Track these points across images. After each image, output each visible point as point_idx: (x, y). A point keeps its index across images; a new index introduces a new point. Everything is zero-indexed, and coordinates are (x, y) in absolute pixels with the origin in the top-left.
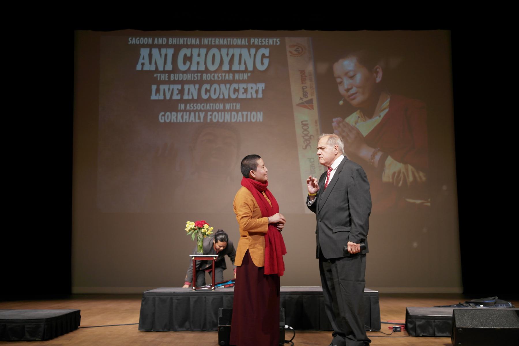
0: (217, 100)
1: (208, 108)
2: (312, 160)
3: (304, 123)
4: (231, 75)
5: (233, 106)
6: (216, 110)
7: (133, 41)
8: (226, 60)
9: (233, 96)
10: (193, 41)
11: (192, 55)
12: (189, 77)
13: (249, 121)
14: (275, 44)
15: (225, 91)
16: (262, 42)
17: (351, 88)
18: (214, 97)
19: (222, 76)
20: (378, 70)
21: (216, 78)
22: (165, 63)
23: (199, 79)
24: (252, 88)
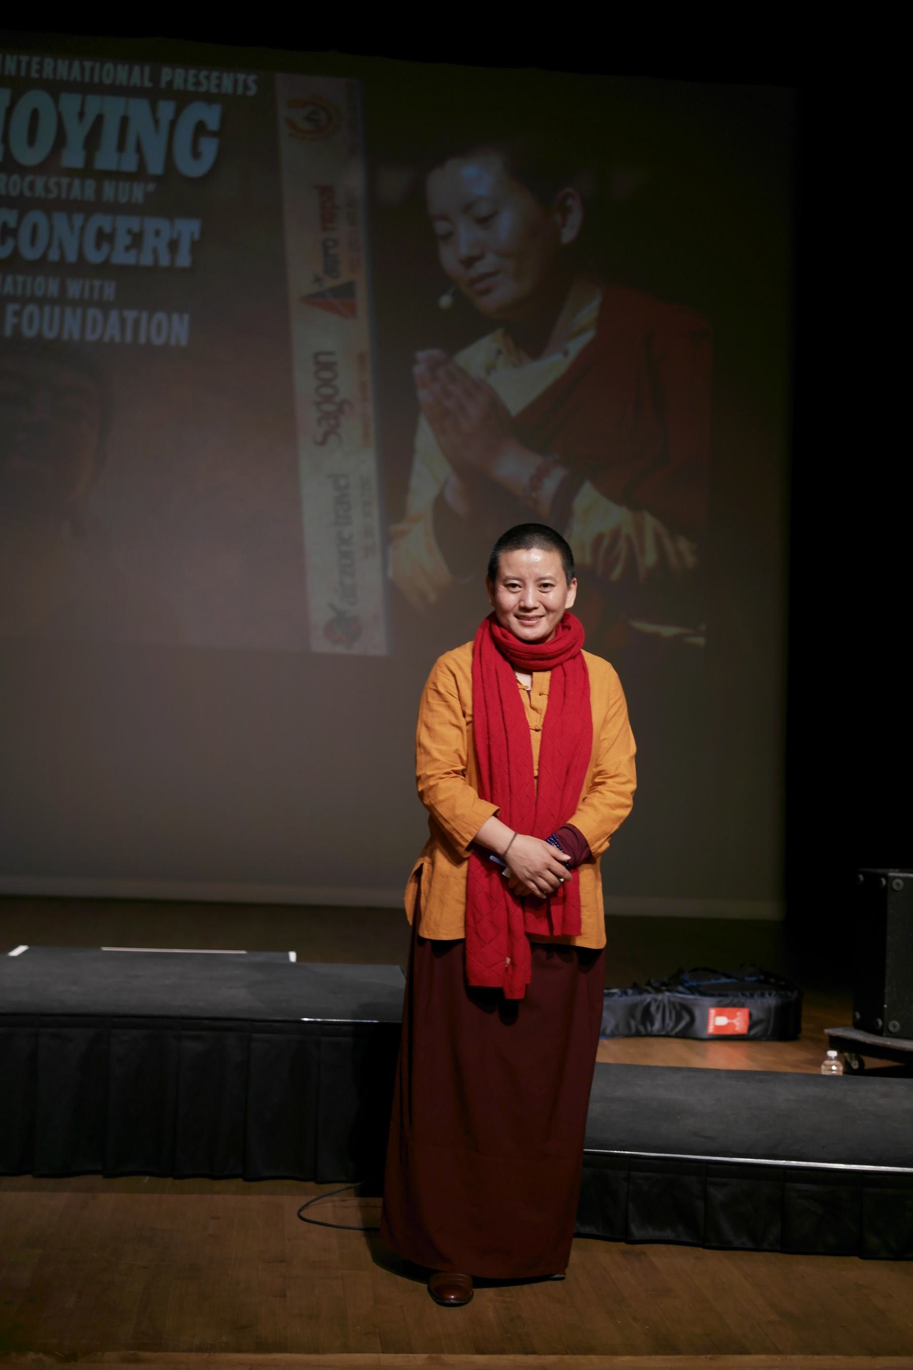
0: (40, 266)
2: (342, 482)
3: (323, 359)
5: (92, 288)
6: (33, 299)
8: (77, 133)
9: (94, 256)
13: (142, 340)
14: (240, 91)
15: (67, 237)
16: (197, 83)
18: (30, 254)
19: (58, 185)
20: (570, 202)
21: (39, 191)
24: (157, 233)
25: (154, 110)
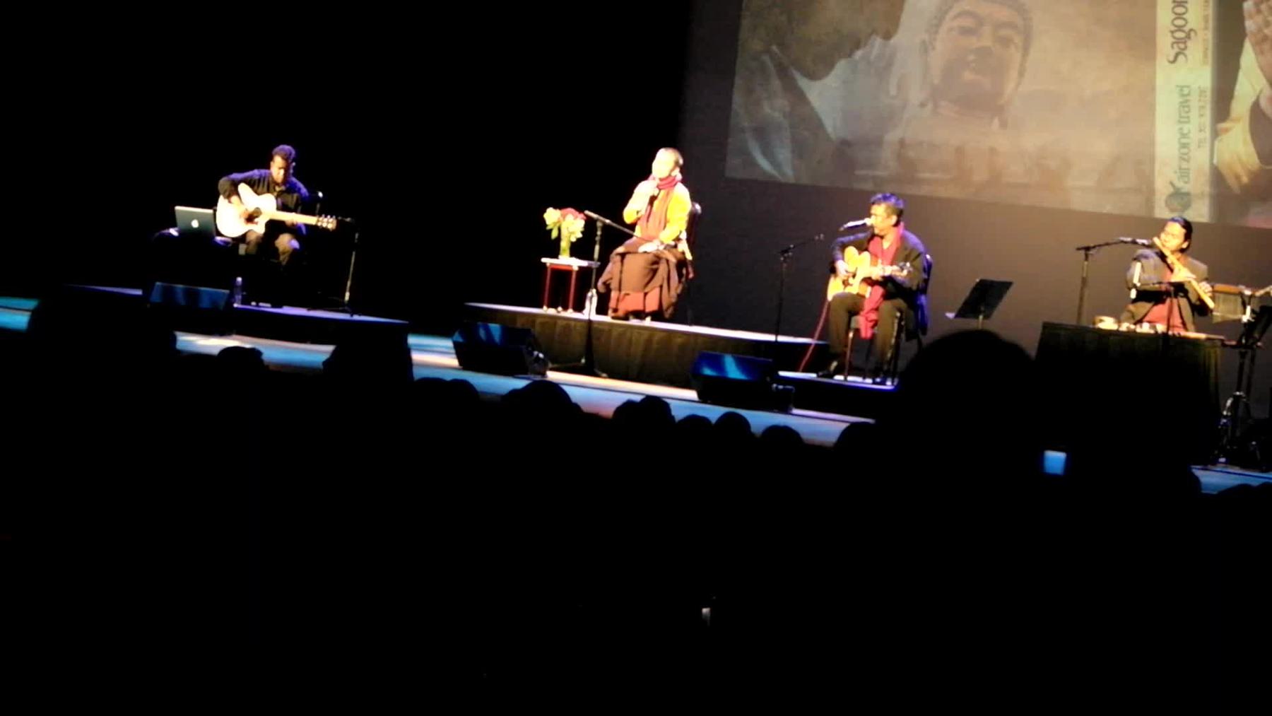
2: (1186, 91)
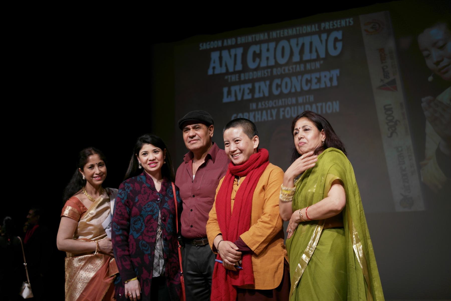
0: (290, 95)
1: (280, 103)
2: (400, 149)
3: (387, 107)
4: (302, 66)
5: (306, 98)
6: (288, 106)
7: (204, 46)
8: (296, 51)
9: (306, 88)
10: (262, 36)
11: (261, 51)
12: (259, 74)
13: (324, 112)
14: (348, 24)
15: (296, 84)
17: (442, 60)
18: (285, 91)
19: (292, 68)
21: (287, 71)
22: (235, 63)
23: (269, 74)
24: (325, 76)
25: (320, 37)
